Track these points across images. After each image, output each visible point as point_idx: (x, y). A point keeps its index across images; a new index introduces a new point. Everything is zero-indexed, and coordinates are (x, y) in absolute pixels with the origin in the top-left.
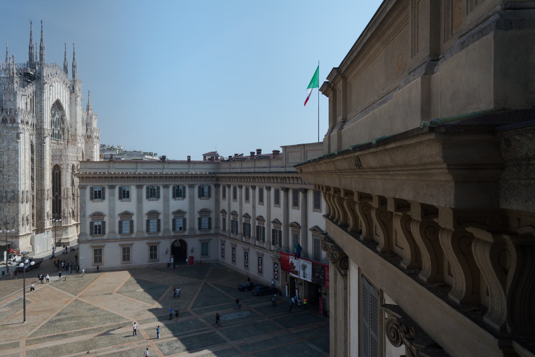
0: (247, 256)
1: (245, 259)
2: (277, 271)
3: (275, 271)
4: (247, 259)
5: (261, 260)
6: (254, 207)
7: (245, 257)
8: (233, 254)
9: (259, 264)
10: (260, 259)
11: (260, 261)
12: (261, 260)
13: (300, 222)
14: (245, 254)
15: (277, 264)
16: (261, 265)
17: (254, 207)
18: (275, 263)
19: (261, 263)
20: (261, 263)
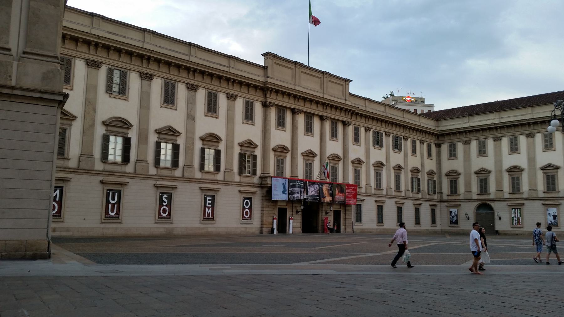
0: (170, 199)
1: (161, 205)
3: (244, 208)
4: (169, 205)
5: (209, 200)
6: (191, 118)
7: (161, 201)
8: (108, 202)
9: (205, 206)
10: (208, 198)
11: (208, 202)
12: (209, 200)
13: (289, 146)
14: (161, 197)
17: (191, 118)
18: (245, 198)
19: (209, 204)
20: (209, 204)
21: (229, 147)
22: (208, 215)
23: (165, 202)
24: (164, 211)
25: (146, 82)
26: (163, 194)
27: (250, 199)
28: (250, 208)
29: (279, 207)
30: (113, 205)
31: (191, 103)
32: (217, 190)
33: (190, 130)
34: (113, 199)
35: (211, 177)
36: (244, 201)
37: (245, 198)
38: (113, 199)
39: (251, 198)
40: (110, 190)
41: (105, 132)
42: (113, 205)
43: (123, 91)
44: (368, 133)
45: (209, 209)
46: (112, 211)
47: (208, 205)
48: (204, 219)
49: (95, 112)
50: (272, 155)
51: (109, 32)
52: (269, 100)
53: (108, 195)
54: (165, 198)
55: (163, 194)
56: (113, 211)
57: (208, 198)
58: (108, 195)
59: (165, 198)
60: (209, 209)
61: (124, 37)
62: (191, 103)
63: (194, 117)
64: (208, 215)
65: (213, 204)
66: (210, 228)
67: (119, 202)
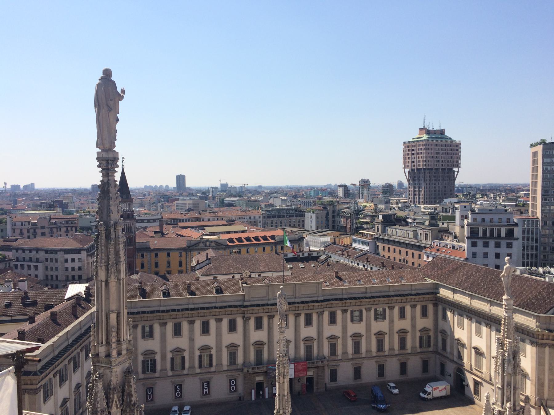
0: (181, 387)
1: (176, 391)
2: (235, 385)
3: (231, 385)
4: (181, 391)
5: (206, 384)
6: (192, 340)
7: (176, 389)
8: (147, 394)
10: (205, 383)
11: (205, 385)
12: (206, 384)
15: (235, 380)
16: (209, 388)
19: (206, 386)
20: (206, 386)
21: (219, 351)
22: (206, 392)
23: (178, 389)
24: (178, 394)
25: (163, 327)
26: (177, 385)
27: (235, 380)
28: (235, 385)
29: (257, 382)
30: (150, 395)
31: (191, 331)
32: (210, 379)
33: (192, 347)
34: (150, 392)
35: (208, 370)
36: (230, 381)
37: (232, 380)
38: (150, 392)
39: (236, 379)
40: (148, 388)
41: (143, 359)
42: (150, 395)
43: (151, 335)
44: (345, 314)
45: (206, 390)
46: (150, 398)
47: (205, 387)
48: (203, 395)
49: (137, 350)
50: (252, 349)
51: (141, 307)
52: (246, 316)
53: (147, 391)
54: (178, 387)
55: (177, 385)
56: (150, 398)
57: (205, 383)
58: (147, 391)
59: (178, 387)
60: (206, 390)
61: (150, 307)
62: (191, 331)
63: (194, 339)
64: (206, 392)
65: (208, 386)
66: (207, 399)
67: (152, 393)
